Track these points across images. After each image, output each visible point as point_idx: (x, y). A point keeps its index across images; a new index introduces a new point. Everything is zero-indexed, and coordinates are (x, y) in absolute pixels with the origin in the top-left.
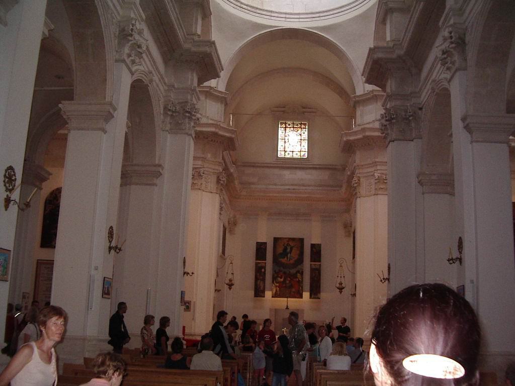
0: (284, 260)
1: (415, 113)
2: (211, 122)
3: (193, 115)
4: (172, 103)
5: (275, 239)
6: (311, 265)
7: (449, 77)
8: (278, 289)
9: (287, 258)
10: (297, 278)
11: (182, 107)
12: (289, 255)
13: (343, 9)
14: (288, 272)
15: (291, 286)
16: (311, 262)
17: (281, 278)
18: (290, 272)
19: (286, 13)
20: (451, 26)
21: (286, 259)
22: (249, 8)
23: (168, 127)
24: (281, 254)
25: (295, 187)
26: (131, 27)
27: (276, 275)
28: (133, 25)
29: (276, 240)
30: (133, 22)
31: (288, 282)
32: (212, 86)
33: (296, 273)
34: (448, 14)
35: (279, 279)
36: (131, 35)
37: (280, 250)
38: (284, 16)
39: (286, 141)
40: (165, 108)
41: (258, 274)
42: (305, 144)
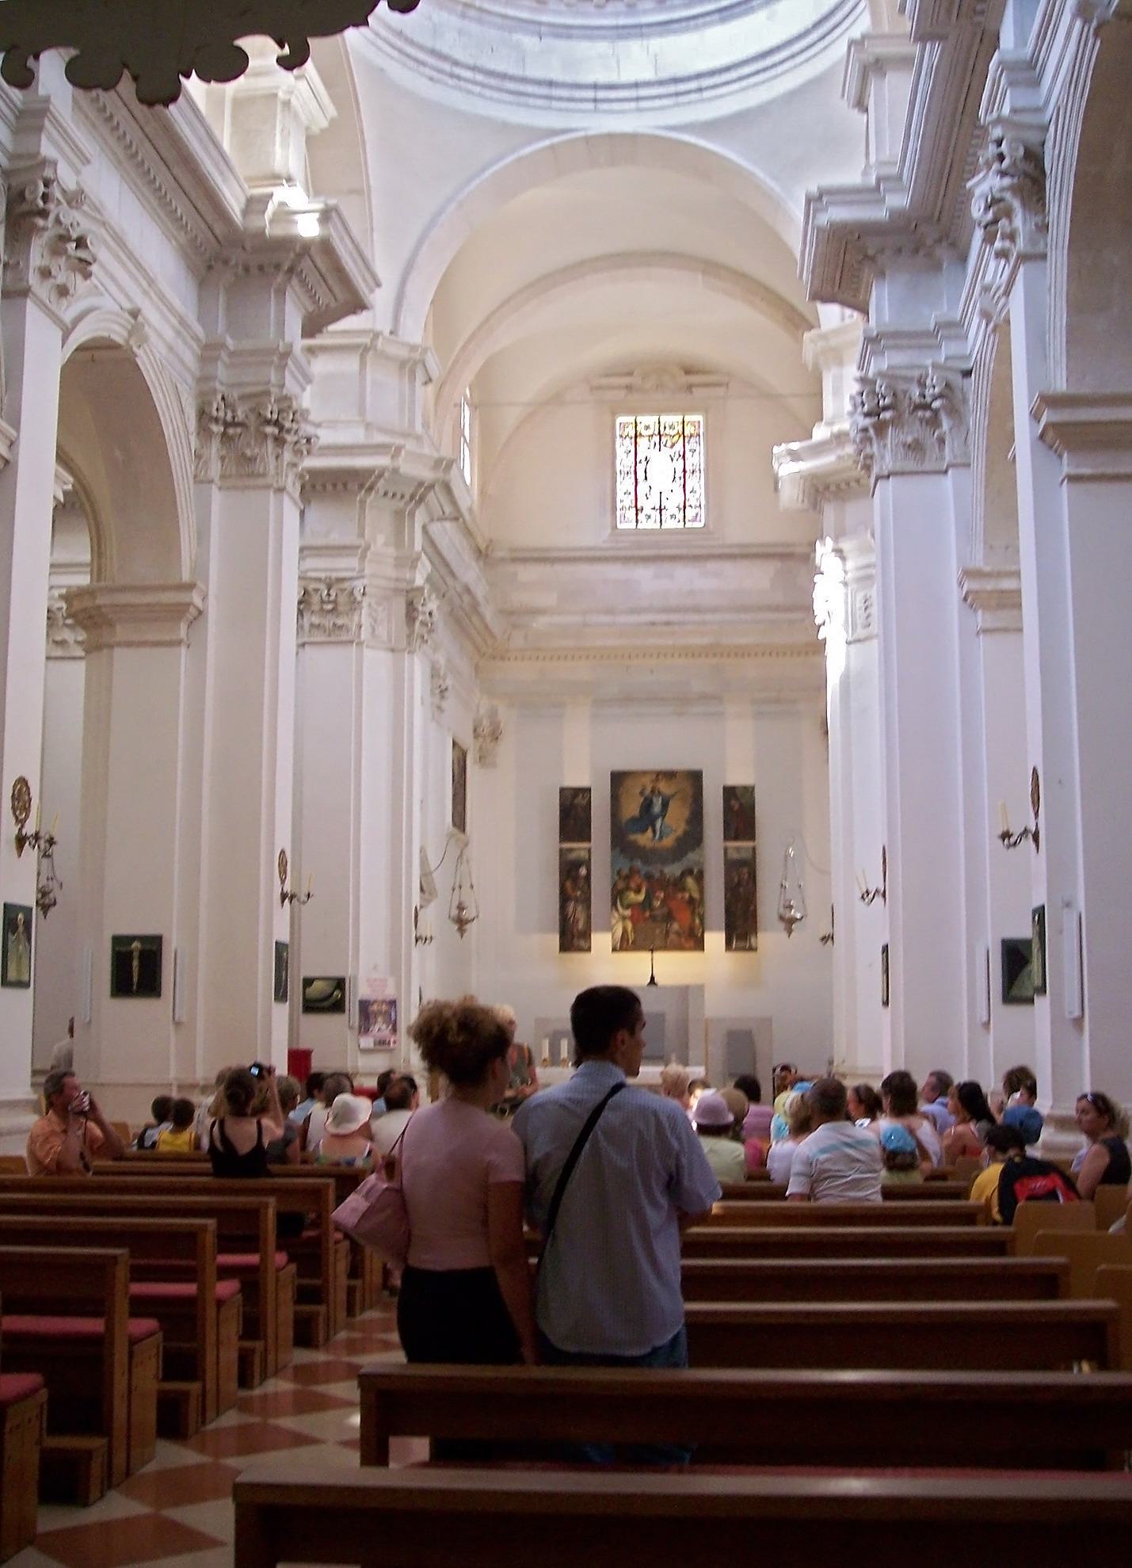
0: (644, 839)
1: (947, 385)
2: (379, 438)
3: (289, 431)
4: (223, 398)
5: (618, 779)
6: (726, 850)
9: (654, 832)
11: (252, 410)
13: (769, 61)
14: (657, 875)
15: (669, 917)
16: (726, 838)
18: (662, 872)
19: (595, 87)
21: (650, 831)
22: (479, 77)
23: (215, 470)
24: (633, 820)
25: (673, 617)
26: (42, 189)
27: (621, 885)
29: (618, 779)
31: (657, 904)
32: (378, 327)
33: (683, 875)
34: (996, 82)
36: (44, 214)
37: (631, 808)
38: (590, 94)
40: (203, 414)
41: (568, 884)
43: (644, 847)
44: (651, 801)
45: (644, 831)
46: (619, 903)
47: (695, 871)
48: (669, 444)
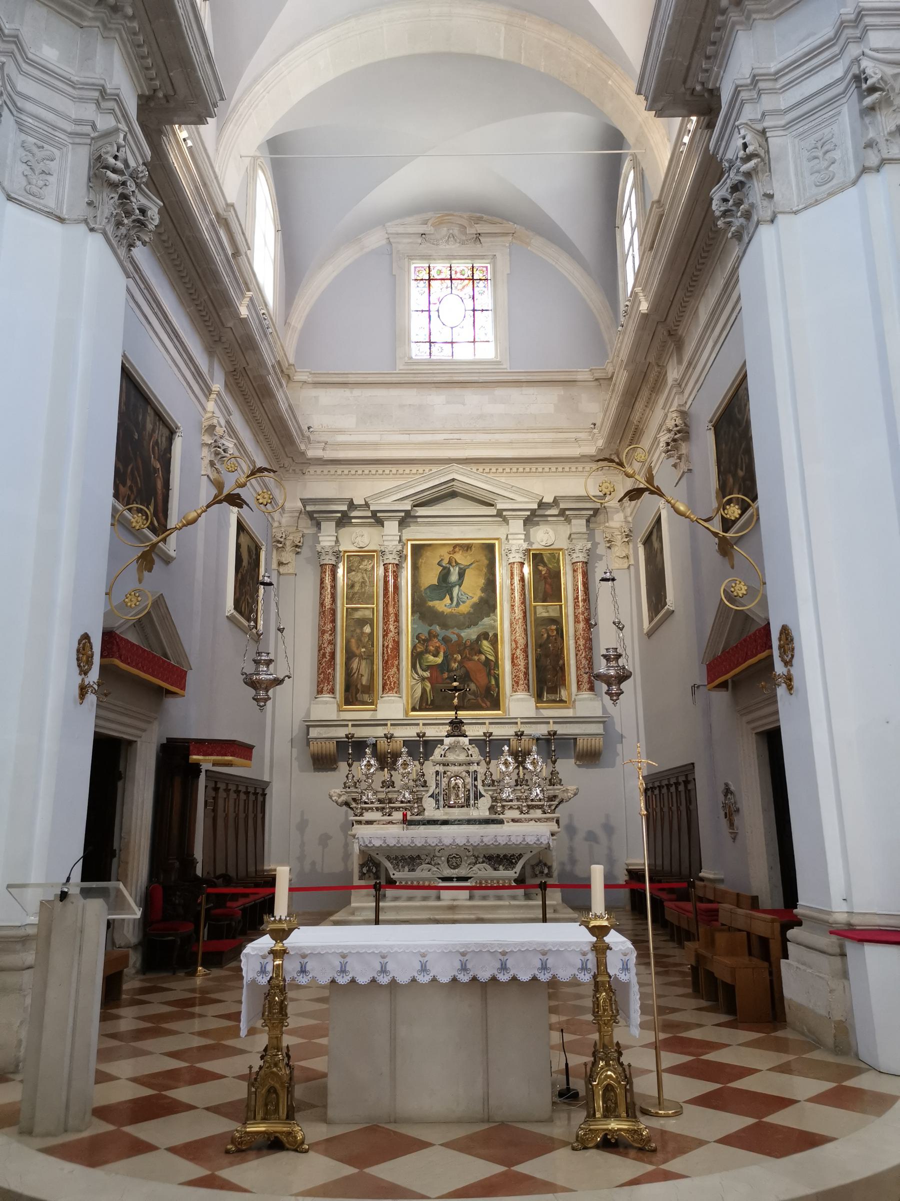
0: (442, 605)
8: (428, 686)
9: (451, 599)
10: (480, 652)
12: (456, 591)
14: (454, 638)
17: (435, 656)
18: (459, 636)
21: (448, 597)
24: (432, 588)
33: (479, 638)
35: (431, 658)
37: (430, 578)
39: (434, 314)
42: (485, 321)
43: (443, 612)
44: (449, 568)
45: (442, 599)
46: (418, 666)
47: (491, 635)
48: (460, 287)
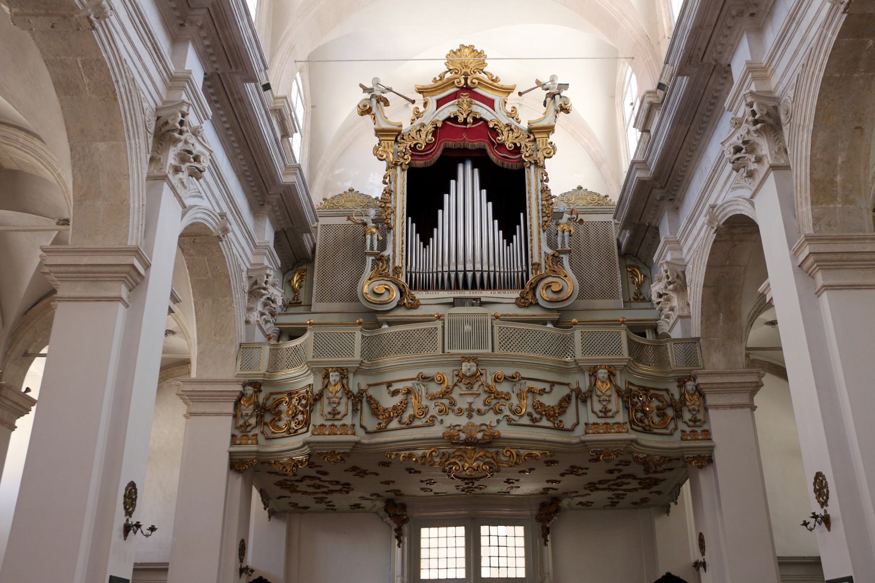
7: (748, 194)
20: (752, 93)
26: (180, 118)
28: (184, 115)
30: (185, 109)
